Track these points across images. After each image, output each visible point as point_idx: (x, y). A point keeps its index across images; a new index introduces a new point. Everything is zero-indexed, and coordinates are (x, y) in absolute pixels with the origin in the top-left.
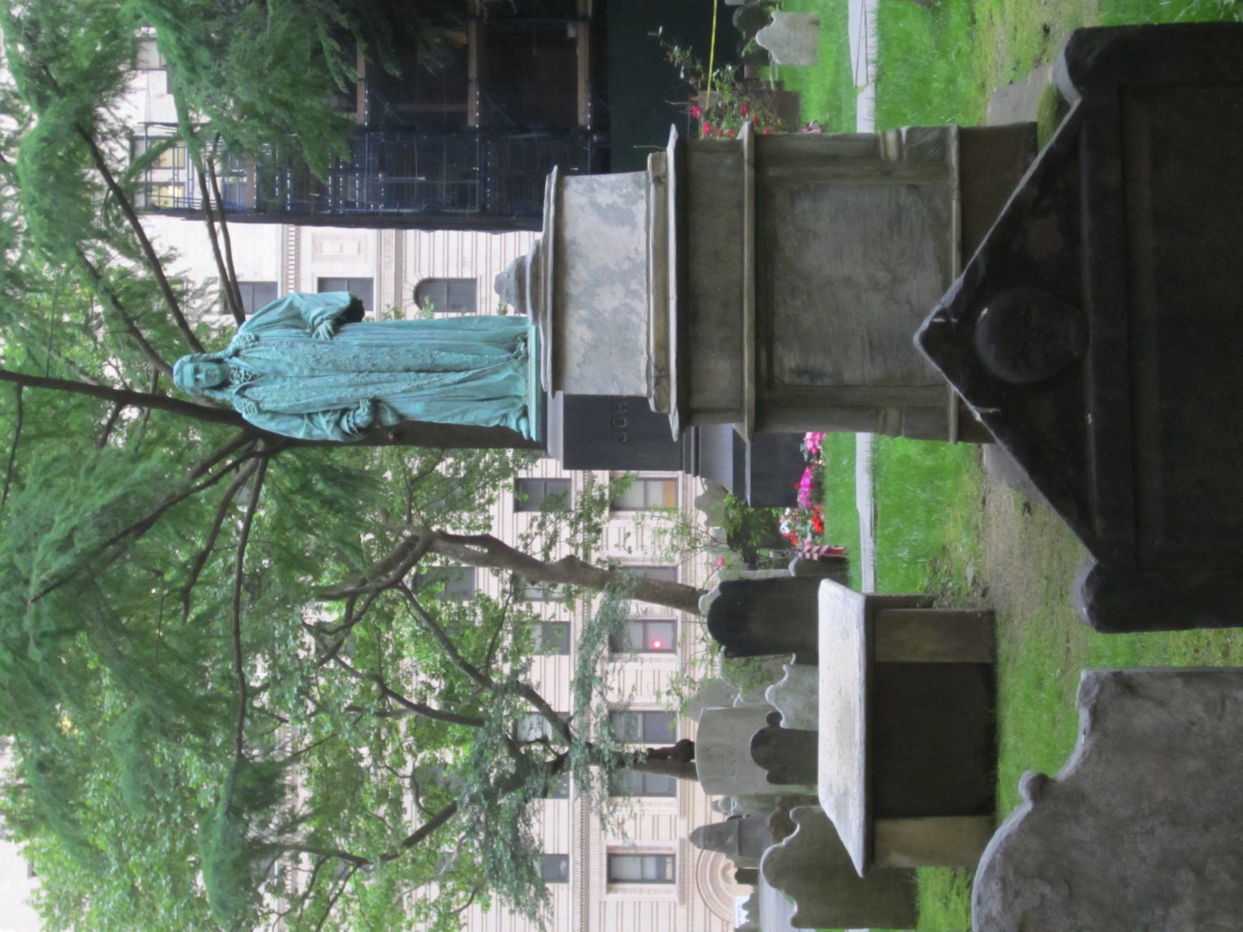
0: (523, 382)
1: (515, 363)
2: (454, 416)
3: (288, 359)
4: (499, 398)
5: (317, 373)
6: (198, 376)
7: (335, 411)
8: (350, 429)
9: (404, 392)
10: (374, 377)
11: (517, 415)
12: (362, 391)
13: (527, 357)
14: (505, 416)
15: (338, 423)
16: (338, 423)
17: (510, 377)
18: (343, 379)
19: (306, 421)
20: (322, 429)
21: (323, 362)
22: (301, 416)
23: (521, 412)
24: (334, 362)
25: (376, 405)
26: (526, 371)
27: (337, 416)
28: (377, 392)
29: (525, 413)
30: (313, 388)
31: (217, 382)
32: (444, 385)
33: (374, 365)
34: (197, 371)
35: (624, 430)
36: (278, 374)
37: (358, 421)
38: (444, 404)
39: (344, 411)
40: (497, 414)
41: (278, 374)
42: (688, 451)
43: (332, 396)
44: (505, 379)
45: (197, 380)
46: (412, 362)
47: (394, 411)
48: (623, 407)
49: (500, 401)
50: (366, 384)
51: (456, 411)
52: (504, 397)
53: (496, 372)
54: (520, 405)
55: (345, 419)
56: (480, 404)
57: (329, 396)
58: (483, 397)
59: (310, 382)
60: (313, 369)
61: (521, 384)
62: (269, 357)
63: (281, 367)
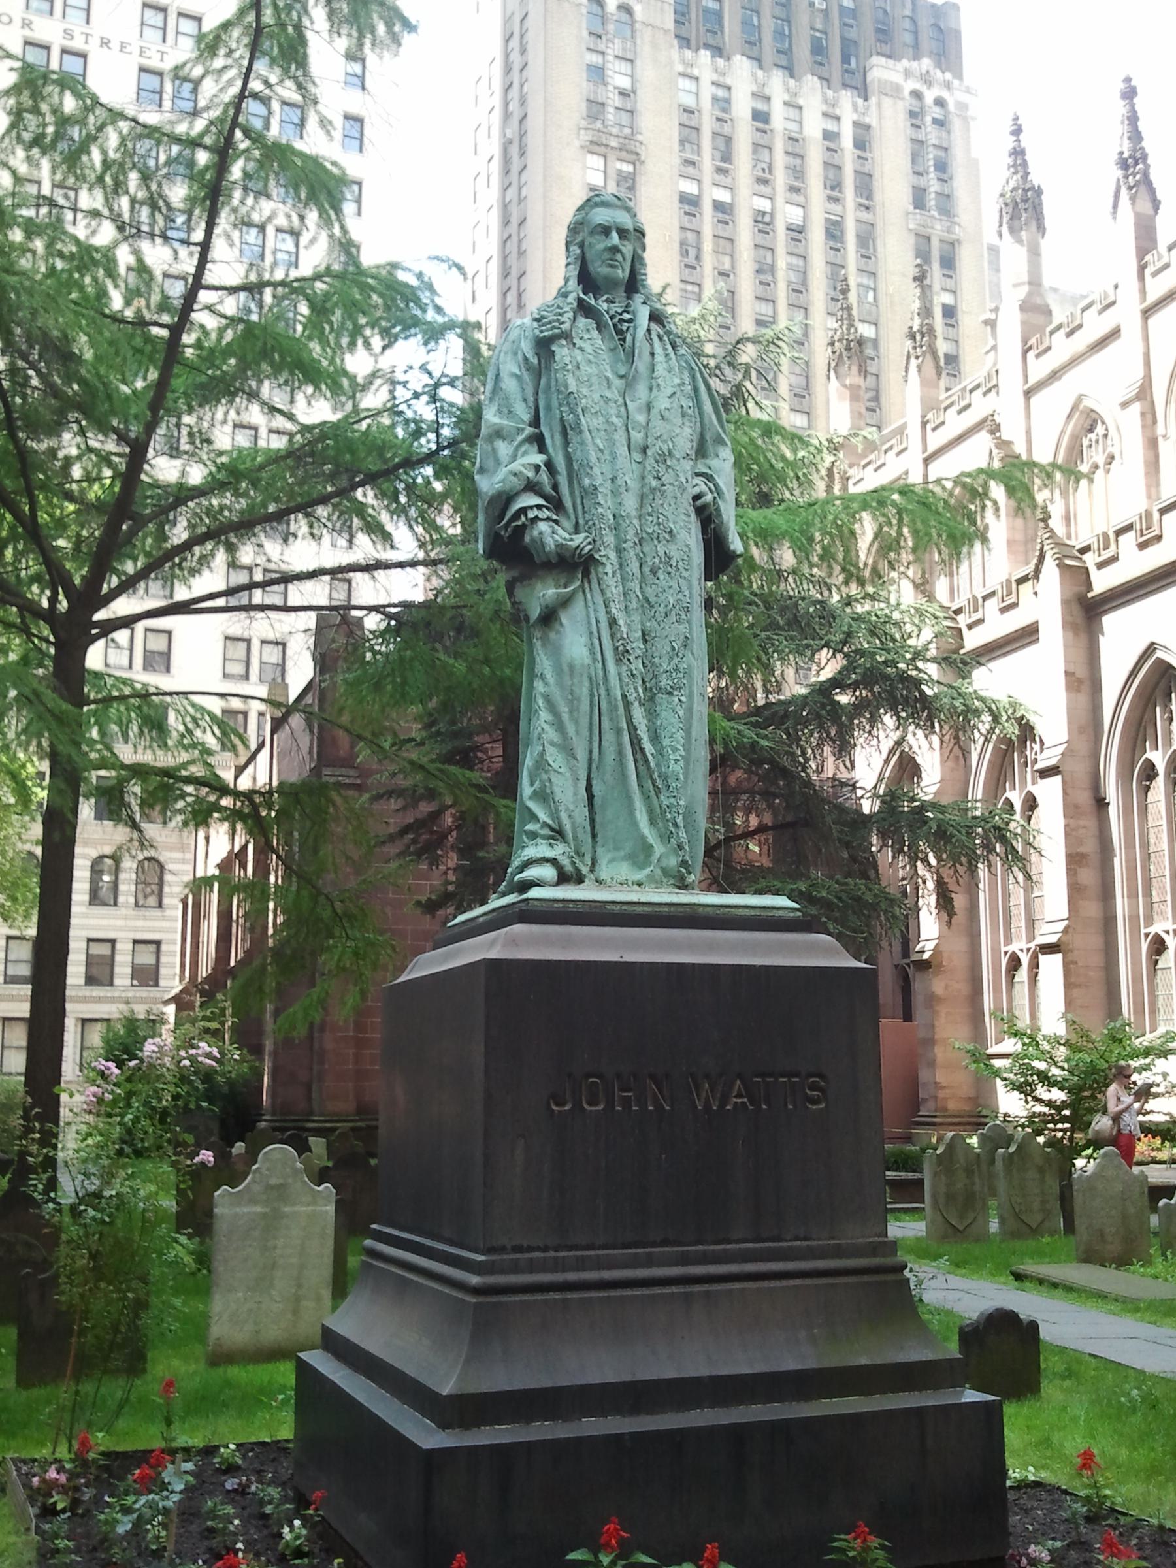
0: (640, 875)
1: (673, 862)
2: (560, 726)
3: (662, 403)
4: (592, 821)
5: (637, 456)
6: (615, 235)
7: (555, 487)
8: (523, 510)
9: (613, 622)
10: (634, 566)
11: (565, 862)
12: (610, 539)
13: (683, 886)
14: (558, 834)
15: (531, 487)
16: (531, 487)
17: (648, 849)
18: (630, 503)
19: (529, 430)
20: (514, 458)
21: (662, 469)
22: (536, 422)
23: (569, 868)
24: (660, 490)
25: (577, 565)
26: (659, 884)
27: (548, 489)
28: (609, 569)
29: (563, 878)
30: (611, 442)
31: (600, 269)
32: (627, 705)
33: (654, 571)
34: (623, 233)
35: (578, 1106)
36: (629, 381)
37: (543, 526)
38: (585, 706)
39: (556, 504)
40: (564, 816)
41: (629, 381)
42: (532, 1267)
43: (598, 475)
44: (643, 838)
45: (606, 231)
46: (661, 647)
47: (565, 602)
48: (626, 1102)
49: (587, 823)
50: (619, 551)
51: (571, 730)
52: (594, 836)
53: (652, 822)
54: (585, 870)
55: (541, 502)
56: (583, 784)
57: (596, 471)
58: (596, 790)
59: (620, 437)
60: (644, 450)
61: (625, 871)
62: (660, 369)
63: (641, 390)
